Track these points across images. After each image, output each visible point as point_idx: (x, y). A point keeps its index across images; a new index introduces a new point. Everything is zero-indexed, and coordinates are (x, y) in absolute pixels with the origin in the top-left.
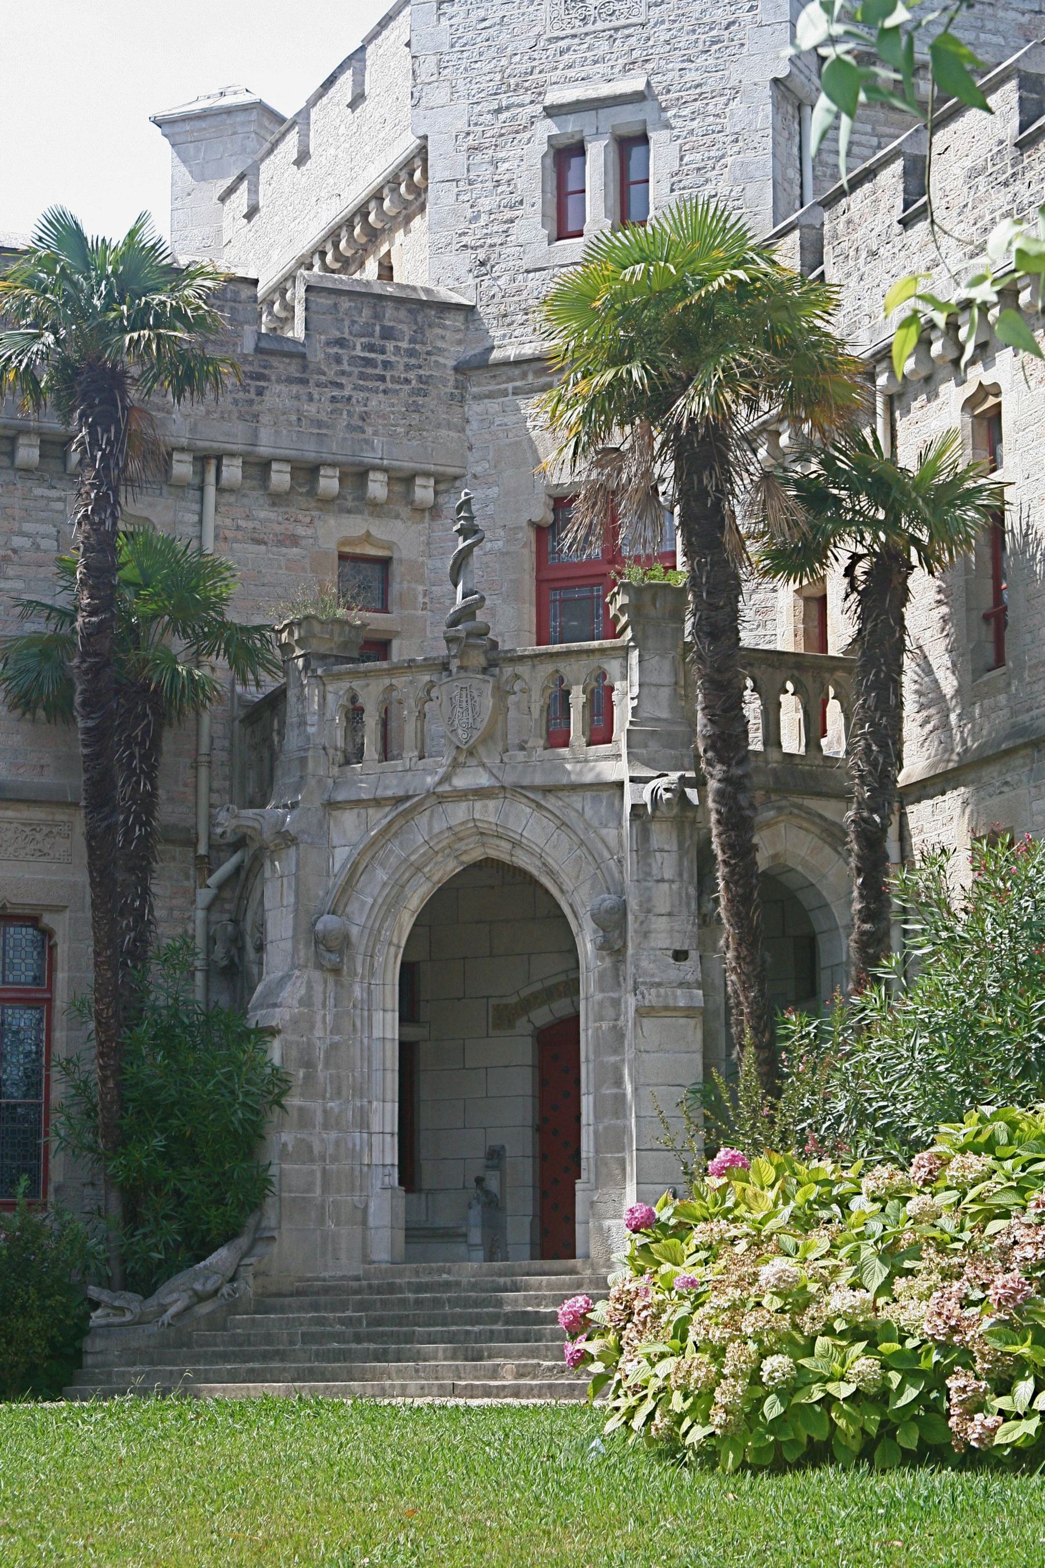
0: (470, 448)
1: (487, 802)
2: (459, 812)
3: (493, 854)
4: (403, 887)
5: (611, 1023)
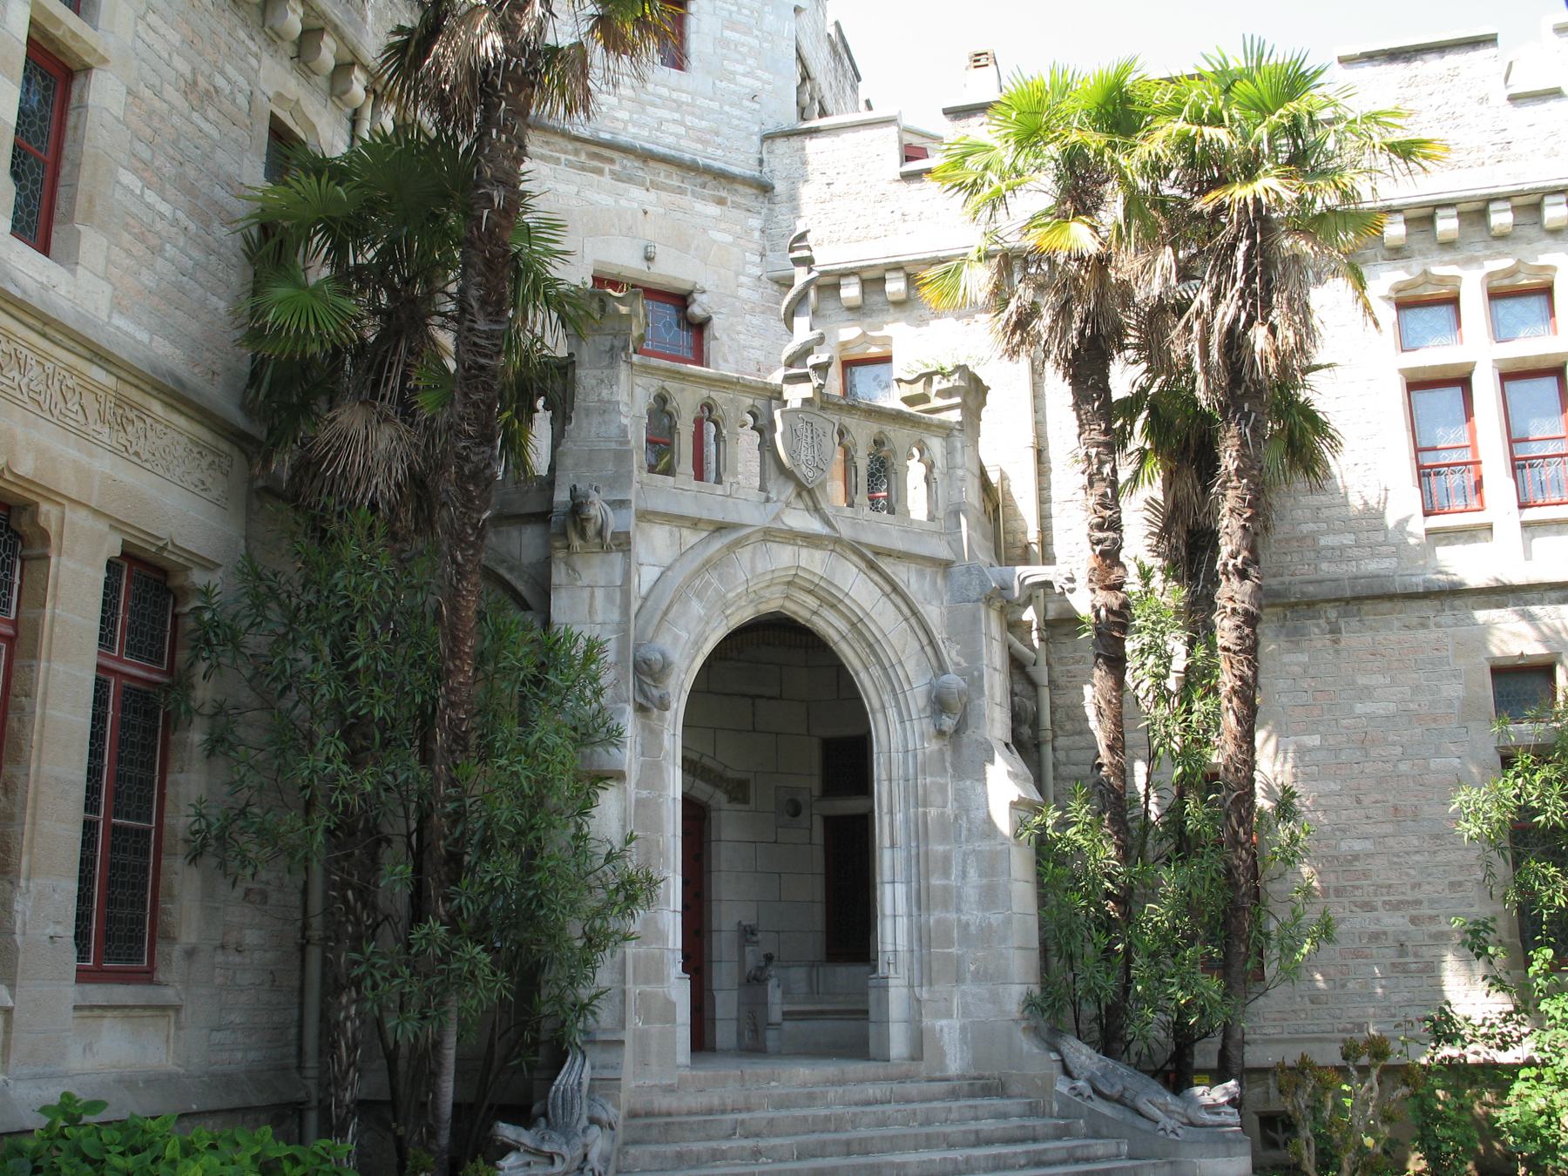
1: (813, 551)
2: (784, 557)
3: (791, 609)
5: (939, 810)
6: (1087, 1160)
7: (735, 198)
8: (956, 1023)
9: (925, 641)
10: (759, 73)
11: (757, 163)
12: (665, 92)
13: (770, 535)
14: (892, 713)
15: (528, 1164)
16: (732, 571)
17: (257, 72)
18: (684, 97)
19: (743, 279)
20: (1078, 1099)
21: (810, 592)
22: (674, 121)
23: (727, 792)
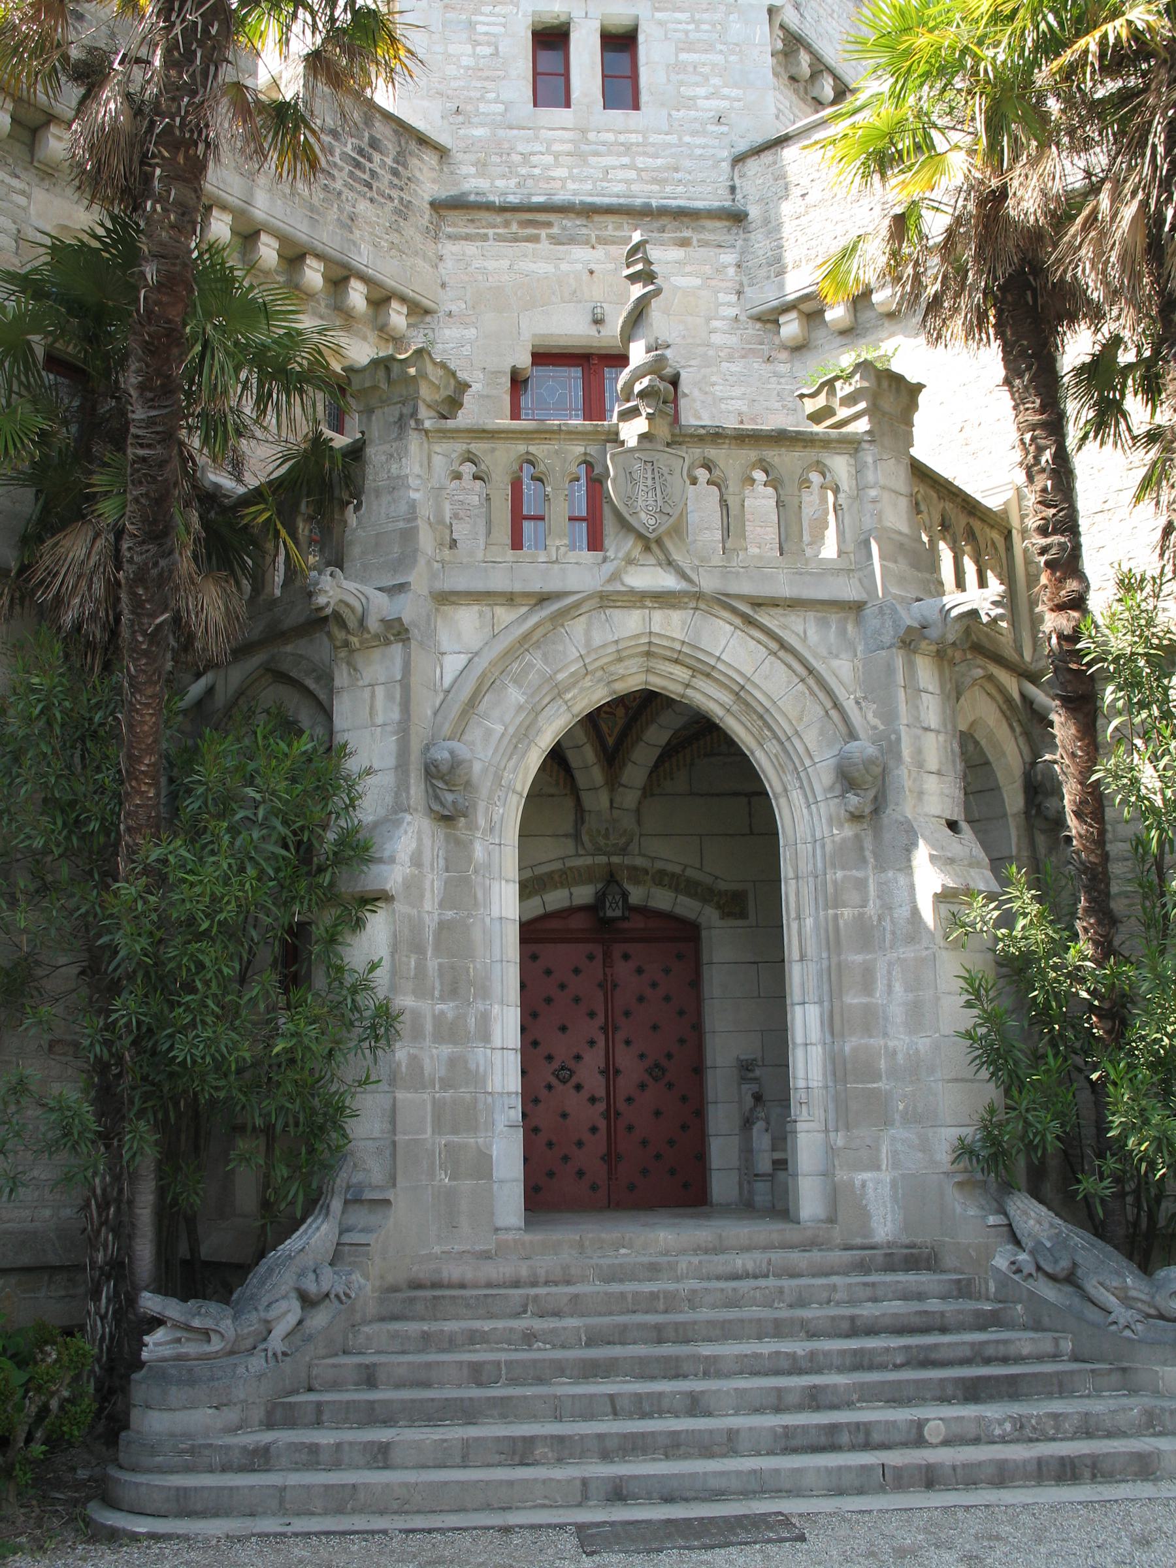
0: (443, 285)
1: (670, 612)
2: (630, 623)
3: (657, 683)
4: (537, 714)
5: (856, 911)
6: (1005, 1360)
7: (702, 236)
8: (886, 1176)
9: (829, 705)
10: (726, 91)
11: (728, 191)
12: (610, 137)
13: (606, 600)
14: (796, 795)
15: (178, 1340)
16: (561, 648)
17: (25, 209)
18: (634, 138)
19: (716, 324)
20: (1016, 1277)
21: (676, 661)
22: (623, 166)
23: (719, 907)
